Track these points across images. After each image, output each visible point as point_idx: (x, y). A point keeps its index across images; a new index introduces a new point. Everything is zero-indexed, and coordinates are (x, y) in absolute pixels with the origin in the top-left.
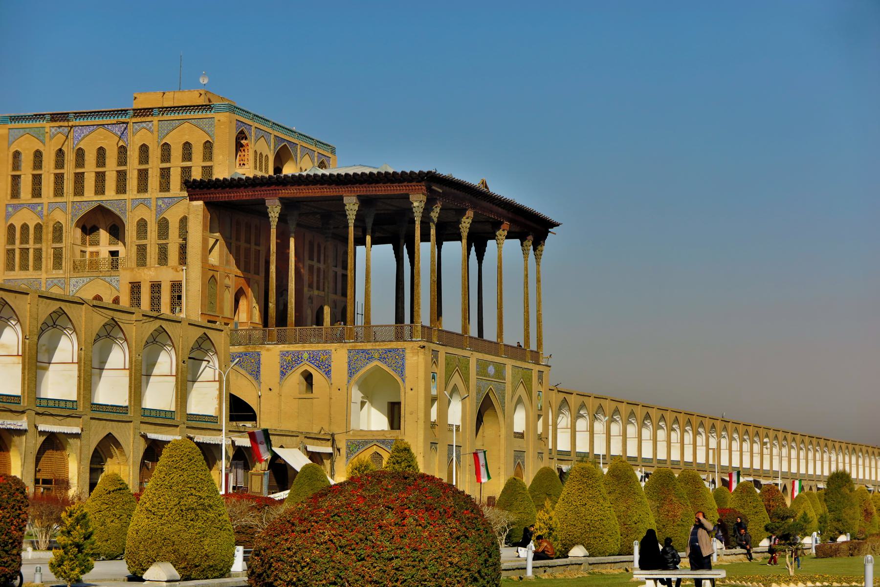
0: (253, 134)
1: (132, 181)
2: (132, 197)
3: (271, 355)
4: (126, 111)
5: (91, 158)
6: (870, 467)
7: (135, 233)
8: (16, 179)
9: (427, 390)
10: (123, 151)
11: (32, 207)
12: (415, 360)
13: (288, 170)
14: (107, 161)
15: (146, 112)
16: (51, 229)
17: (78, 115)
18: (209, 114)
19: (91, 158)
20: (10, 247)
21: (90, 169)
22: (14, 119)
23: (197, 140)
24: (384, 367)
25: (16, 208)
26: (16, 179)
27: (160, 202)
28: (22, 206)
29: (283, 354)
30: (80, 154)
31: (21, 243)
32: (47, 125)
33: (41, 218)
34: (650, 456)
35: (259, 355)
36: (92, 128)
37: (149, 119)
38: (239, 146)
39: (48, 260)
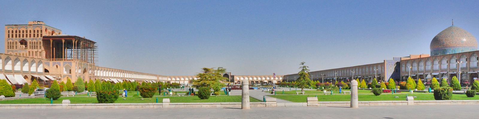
3: (51, 63)
5: (21, 32)
8: (9, 35)
9: (75, 68)
13: (54, 35)
15: (31, 25)
17: (19, 25)
19: (21, 32)
22: (8, 25)
23: (39, 29)
26: (9, 35)
28: (10, 39)
29: (53, 62)
30: (20, 31)
32: (14, 26)
38: (46, 31)
39: (15, 47)
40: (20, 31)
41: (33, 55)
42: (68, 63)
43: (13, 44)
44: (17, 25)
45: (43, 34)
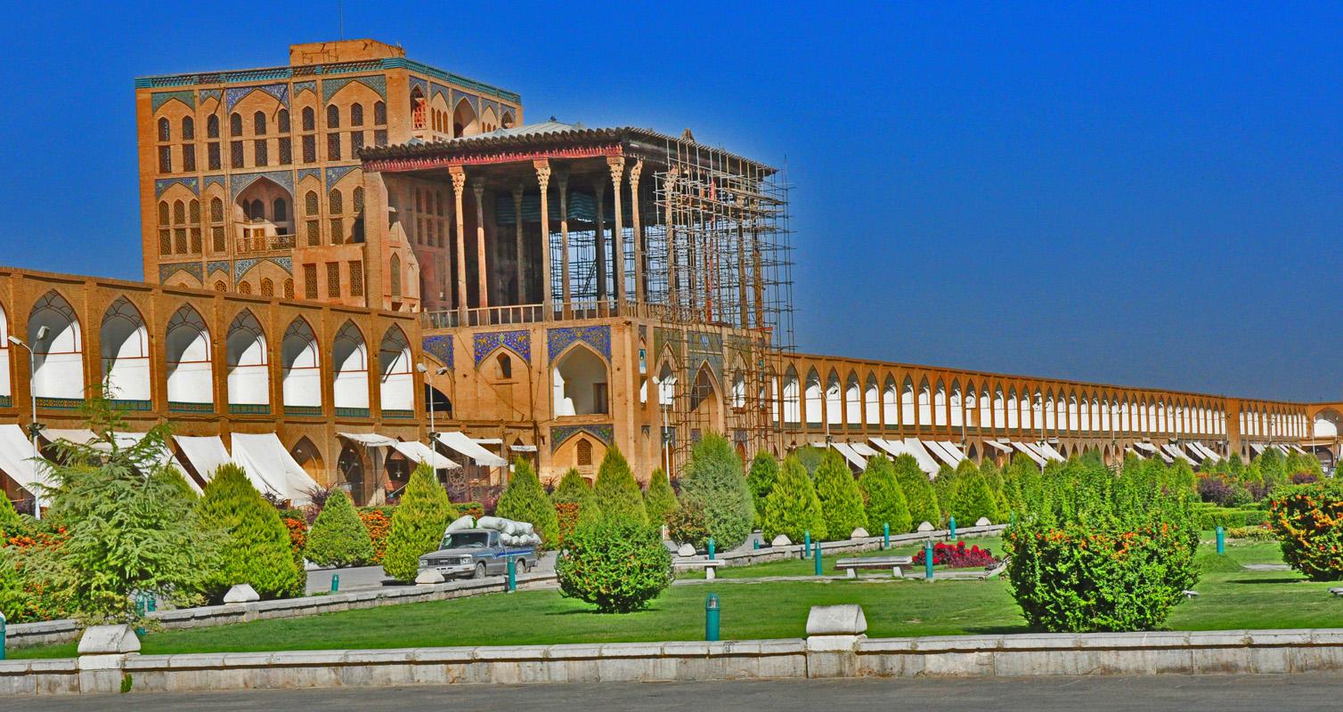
0: (429, 89)
1: (297, 150)
2: (298, 167)
4: (284, 69)
5: (248, 124)
7: (304, 208)
8: (164, 151)
9: (635, 369)
11: (186, 182)
13: (471, 133)
16: (209, 205)
17: (230, 75)
21: (248, 138)
23: (368, 99)
24: (588, 347)
25: (169, 183)
28: (174, 181)
29: (477, 337)
31: (177, 222)
33: (197, 194)
34: (912, 422)
35: (451, 338)
36: (247, 90)
37: (311, 78)
38: (415, 106)
39: (209, 242)
41: (334, 290)
42: (583, 338)
43: (196, 217)
44: (215, 78)
45: (390, 134)
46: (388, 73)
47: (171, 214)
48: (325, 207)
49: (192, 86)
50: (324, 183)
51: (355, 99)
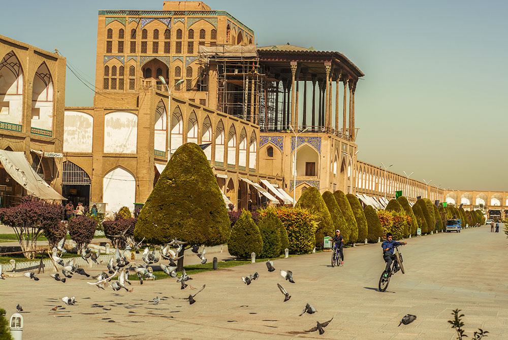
5: (150, 35)
6: (384, 184)
7: (174, 74)
8: (109, 44)
10: (168, 33)
11: (117, 57)
12: (326, 144)
14: (159, 36)
15: (182, 13)
18: (215, 16)
19: (150, 35)
20: (106, 77)
21: (150, 40)
23: (208, 28)
24: (311, 146)
25: (110, 58)
26: (109, 44)
27: (188, 59)
28: (114, 57)
30: (145, 32)
36: (151, 19)
37: (183, 16)
40: (145, 32)
44: (136, 12)
46: (219, 17)
47: (110, 72)
48: (184, 74)
49: (125, 15)
50: (184, 64)
51: (202, 27)
